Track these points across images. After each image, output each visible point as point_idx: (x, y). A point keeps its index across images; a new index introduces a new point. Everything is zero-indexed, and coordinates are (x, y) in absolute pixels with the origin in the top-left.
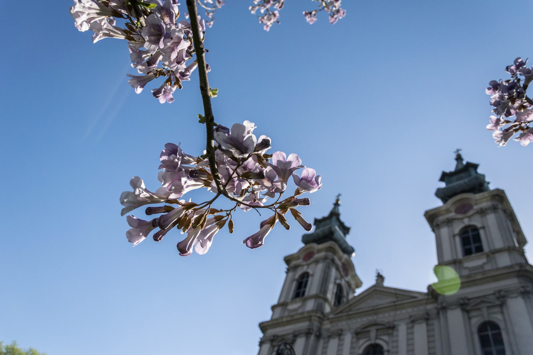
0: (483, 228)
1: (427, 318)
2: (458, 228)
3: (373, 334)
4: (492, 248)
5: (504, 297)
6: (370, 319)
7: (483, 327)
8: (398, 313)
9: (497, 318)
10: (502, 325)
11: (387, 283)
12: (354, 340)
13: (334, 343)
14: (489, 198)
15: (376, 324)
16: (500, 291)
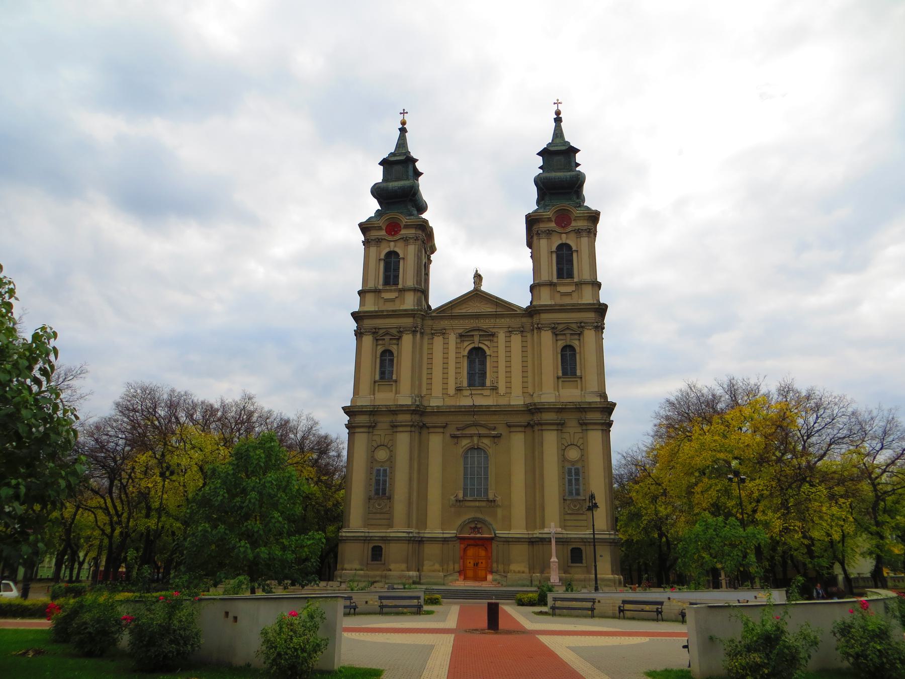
0: (577, 251)
2: (556, 242)
3: (476, 339)
5: (582, 327)
6: (472, 324)
7: (564, 348)
8: (498, 320)
9: (576, 343)
11: (485, 287)
12: (459, 341)
13: (438, 341)
15: (479, 330)
16: (581, 323)
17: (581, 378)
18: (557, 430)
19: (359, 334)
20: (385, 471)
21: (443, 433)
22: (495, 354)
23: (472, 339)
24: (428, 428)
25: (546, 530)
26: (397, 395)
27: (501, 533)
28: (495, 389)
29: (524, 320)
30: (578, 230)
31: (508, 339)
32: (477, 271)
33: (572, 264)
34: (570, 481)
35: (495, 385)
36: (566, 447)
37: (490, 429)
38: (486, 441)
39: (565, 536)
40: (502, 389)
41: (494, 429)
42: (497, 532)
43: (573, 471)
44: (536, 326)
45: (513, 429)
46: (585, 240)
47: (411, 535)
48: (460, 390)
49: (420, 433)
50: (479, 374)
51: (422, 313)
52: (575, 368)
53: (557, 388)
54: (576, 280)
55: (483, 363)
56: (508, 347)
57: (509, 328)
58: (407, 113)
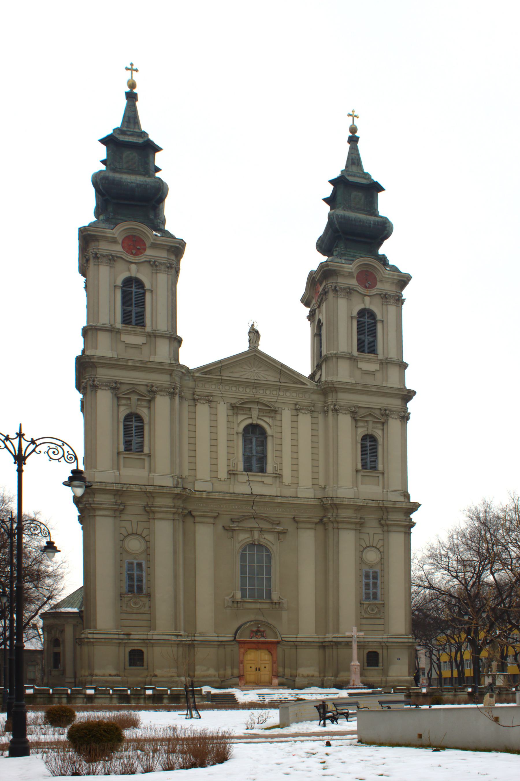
21: (214, 524)
22: (278, 435)
23: (247, 412)
26: (152, 474)
28: (278, 476)
29: (315, 397)
30: (385, 295)
31: (295, 418)
36: (365, 549)
37: (273, 524)
38: (269, 537)
40: (287, 478)
41: (278, 524)
45: (300, 525)
48: (234, 474)
50: (257, 457)
56: (295, 428)
57: (296, 405)
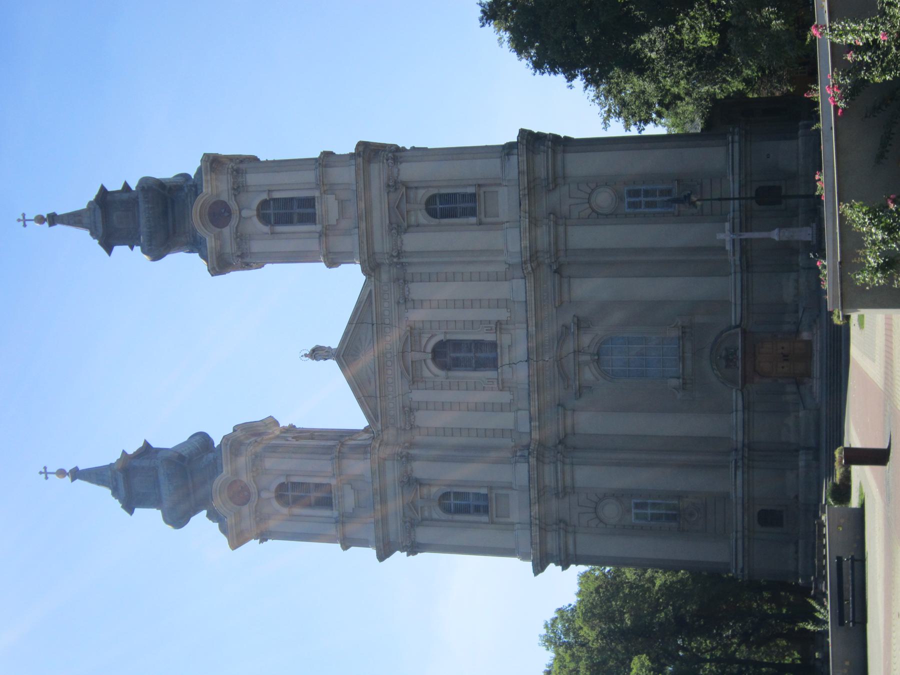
1: (403, 281)
4: (270, 197)
5: (396, 182)
9: (422, 195)
10: (434, 191)
11: (334, 342)
14: (214, 176)
16: (389, 186)
17: (479, 186)
18: (566, 225)
19: (413, 549)
20: (637, 506)
24: (566, 435)
25: (728, 247)
27: (734, 316)
28: (499, 326)
29: (385, 277)
30: (234, 189)
32: (306, 355)
33: (292, 199)
34: (649, 205)
35: (493, 326)
39: (737, 214)
40: (502, 314)
42: (733, 323)
43: (632, 200)
44: (395, 260)
46: (253, 179)
47: (740, 464)
48: (503, 383)
49: (575, 448)
51: (377, 446)
52: (464, 195)
53: (497, 225)
54: (317, 194)
55: (457, 345)
58: (45, 468)
